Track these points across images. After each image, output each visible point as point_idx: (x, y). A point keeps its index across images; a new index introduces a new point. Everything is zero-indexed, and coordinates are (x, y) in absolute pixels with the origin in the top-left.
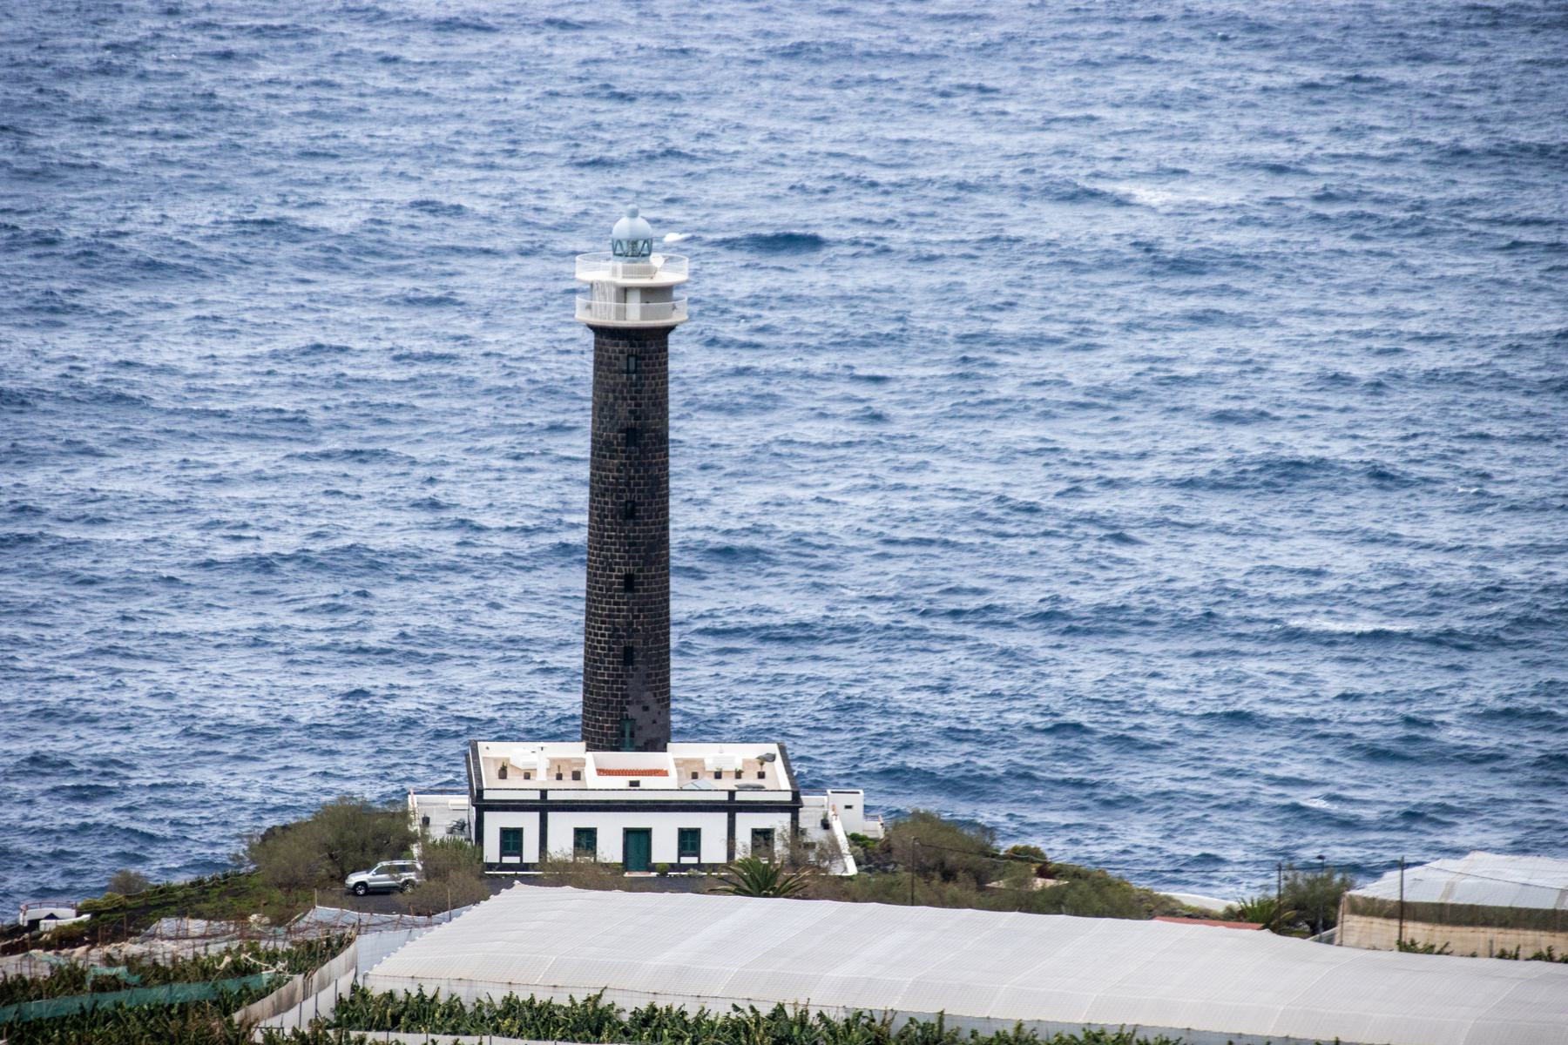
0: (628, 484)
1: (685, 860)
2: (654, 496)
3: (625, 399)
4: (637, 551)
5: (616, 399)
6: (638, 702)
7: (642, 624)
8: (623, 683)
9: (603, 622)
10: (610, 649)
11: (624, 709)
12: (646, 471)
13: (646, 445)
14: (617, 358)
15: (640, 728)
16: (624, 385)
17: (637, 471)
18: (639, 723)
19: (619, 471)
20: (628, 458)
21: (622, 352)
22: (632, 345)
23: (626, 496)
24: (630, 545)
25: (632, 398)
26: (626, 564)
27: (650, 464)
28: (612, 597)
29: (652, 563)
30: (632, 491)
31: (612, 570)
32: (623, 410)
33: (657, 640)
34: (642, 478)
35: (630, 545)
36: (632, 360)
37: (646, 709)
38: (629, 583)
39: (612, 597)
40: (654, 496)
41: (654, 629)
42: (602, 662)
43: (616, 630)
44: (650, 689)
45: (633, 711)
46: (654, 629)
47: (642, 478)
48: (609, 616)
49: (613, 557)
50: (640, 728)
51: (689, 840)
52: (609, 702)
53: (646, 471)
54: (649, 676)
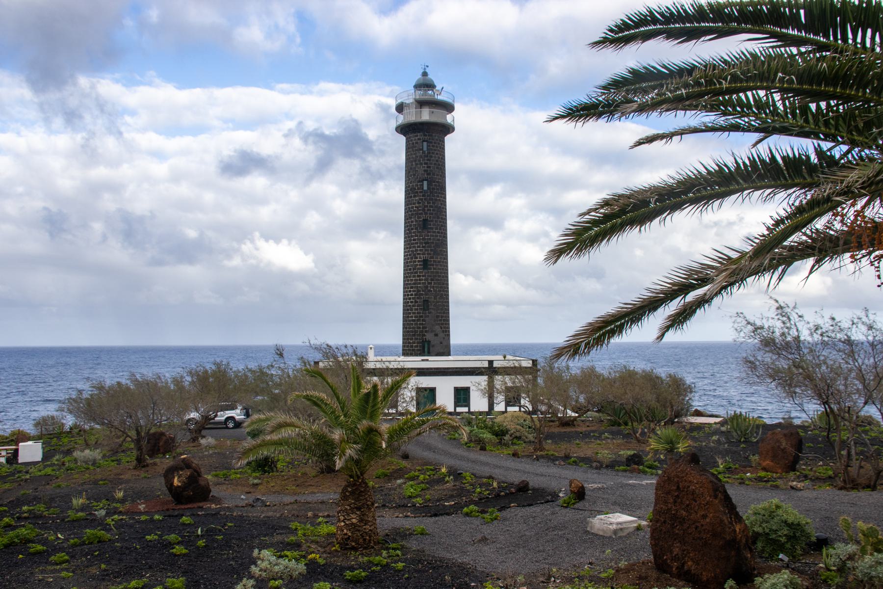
0: (424, 210)
1: (459, 410)
2: (438, 218)
3: (421, 164)
4: (430, 247)
6: (432, 331)
9: (412, 288)
10: (416, 302)
12: (434, 203)
13: (433, 189)
15: (433, 346)
16: (421, 157)
17: (429, 203)
18: (432, 343)
19: (419, 203)
20: (423, 196)
22: (425, 135)
23: (423, 217)
24: (426, 243)
26: (424, 254)
28: (416, 273)
29: (438, 254)
30: (426, 214)
32: (421, 170)
33: (441, 297)
35: (427, 243)
36: (425, 144)
37: (436, 335)
38: (425, 263)
39: (416, 273)
40: (438, 218)
41: (440, 291)
42: (411, 310)
43: (419, 291)
44: (439, 324)
45: (429, 336)
46: (440, 291)
48: (414, 284)
49: (416, 250)
50: (433, 346)
51: (462, 396)
52: (416, 332)
53: (434, 203)
54: (438, 317)
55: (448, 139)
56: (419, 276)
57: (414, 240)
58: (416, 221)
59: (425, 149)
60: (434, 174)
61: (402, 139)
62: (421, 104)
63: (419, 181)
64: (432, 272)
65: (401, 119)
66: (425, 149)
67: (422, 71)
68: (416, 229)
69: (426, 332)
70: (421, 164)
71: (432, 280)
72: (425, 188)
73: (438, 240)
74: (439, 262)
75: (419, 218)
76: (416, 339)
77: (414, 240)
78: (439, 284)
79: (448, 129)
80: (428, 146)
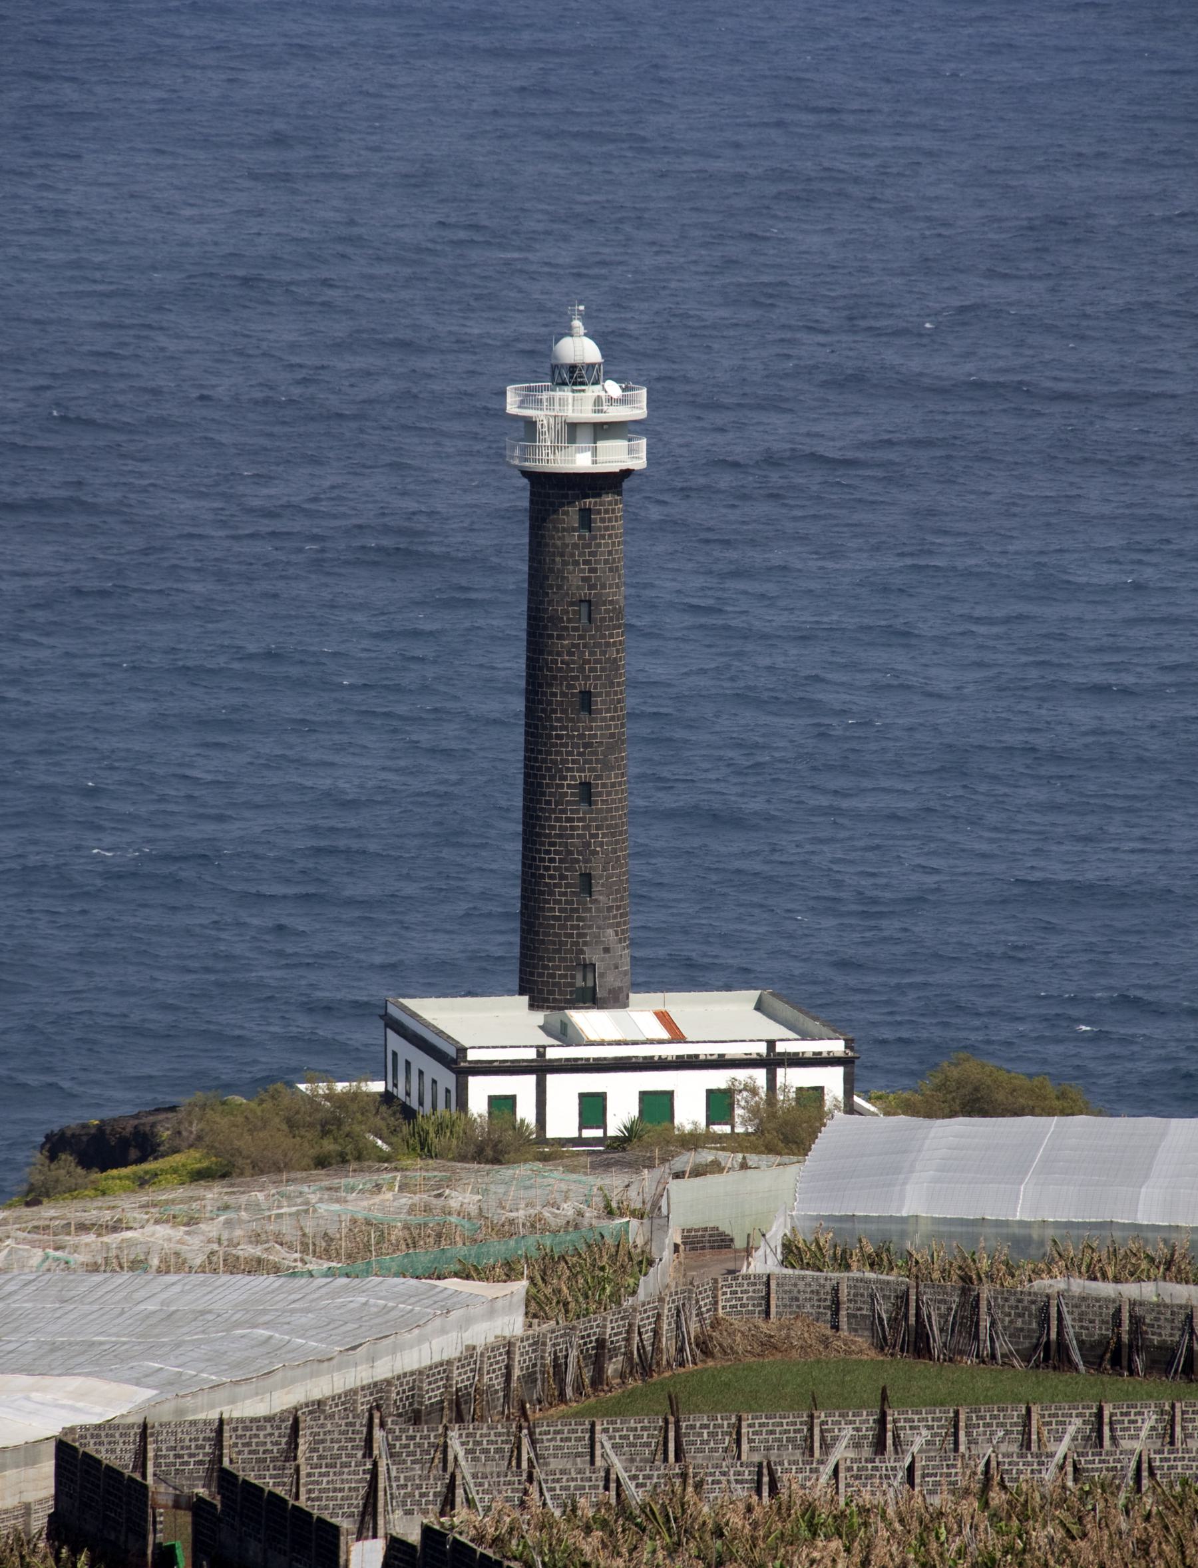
2: (612, 685)
7: (601, 844)
8: (579, 919)
10: (562, 877)
11: (582, 952)
17: (592, 653)
19: (570, 654)
20: (581, 637)
26: (582, 770)
27: (608, 644)
28: (564, 811)
29: (613, 768)
31: (565, 778)
34: (597, 661)
37: (607, 950)
41: (615, 851)
43: (570, 853)
44: (610, 926)
46: (615, 851)
47: (597, 661)
53: (603, 653)
60: (603, 587)
64: (599, 811)
69: (585, 944)
70: (577, 563)
71: (598, 828)
73: (612, 736)
74: (613, 785)
75: (570, 687)
78: (613, 835)
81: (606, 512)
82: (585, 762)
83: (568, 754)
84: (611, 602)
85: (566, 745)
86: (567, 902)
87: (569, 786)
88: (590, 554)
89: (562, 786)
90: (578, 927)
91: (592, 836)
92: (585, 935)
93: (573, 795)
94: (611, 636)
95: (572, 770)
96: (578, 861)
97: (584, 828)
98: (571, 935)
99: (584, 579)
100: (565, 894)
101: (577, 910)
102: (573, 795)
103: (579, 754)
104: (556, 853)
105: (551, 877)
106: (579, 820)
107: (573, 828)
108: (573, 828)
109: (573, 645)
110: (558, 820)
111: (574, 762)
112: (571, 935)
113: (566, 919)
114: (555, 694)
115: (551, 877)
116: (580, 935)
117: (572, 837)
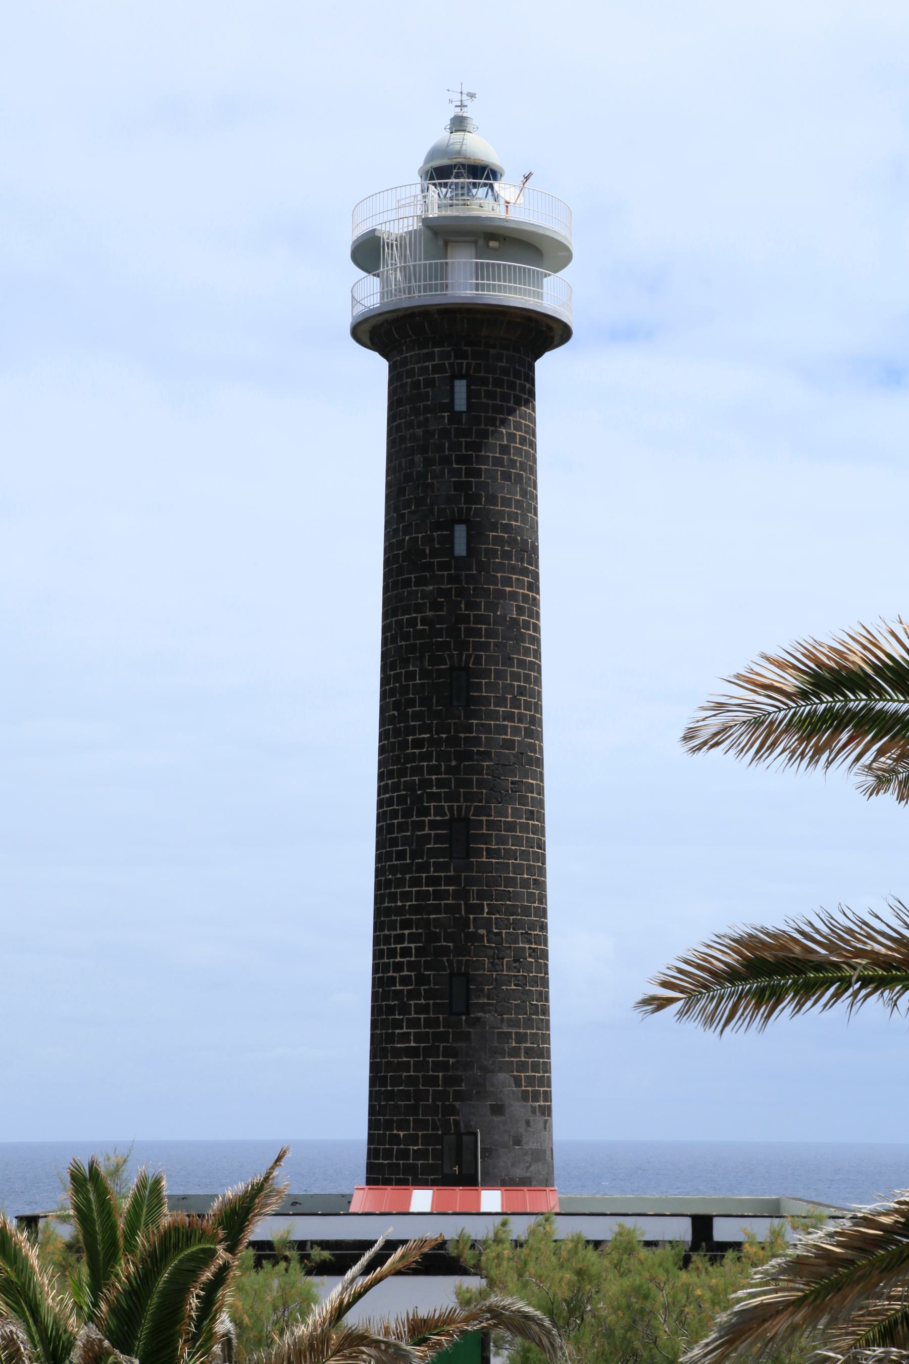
3: (446, 461)
5: (428, 462)
8: (448, 1052)
9: (406, 924)
10: (421, 979)
11: (453, 1111)
14: (430, 383)
19: (436, 606)
20: (452, 579)
21: (437, 369)
25: (459, 460)
26: (452, 797)
28: (424, 868)
31: (425, 812)
36: (461, 387)
40: (508, 661)
55: (549, 369)
56: (431, 881)
57: (418, 744)
58: (425, 674)
59: (460, 404)
61: (375, 369)
62: (443, 236)
63: (438, 526)
65: (371, 293)
66: (460, 404)
67: (453, 112)
68: (424, 701)
69: (459, 1096)
70: (446, 461)
71: (481, 895)
72: (460, 549)
74: (511, 827)
76: (419, 1124)
77: (418, 744)
79: (548, 332)
80: (470, 394)
81: (498, 383)
82: (460, 783)
83: (433, 770)
84: (507, 528)
85: (426, 757)
86: (429, 1023)
87: (433, 825)
88: (469, 446)
89: (420, 826)
90: (445, 1067)
91: (471, 909)
92: (457, 1081)
93: (439, 839)
94: (508, 582)
95: (435, 797)
96: (445, 951)
97: (456, 895)
98: (433, 1081)
99: (458, 486)
100: (424, 1009)
101: (443, 1037)
102: (439, 839)
103: (449, 770)
104: (413, 938)
105: (405, 981)
106: (449, 881)
107: (438, 895)
108: (438, 895)
109: (441, 593)
110: (416, 882)
111: (440, 783)
112: (433, 1081)
113: (428, 1052)
114: (411, 676)
115: (405, 981)
116: (448, 1081)
117: (437, 909)
